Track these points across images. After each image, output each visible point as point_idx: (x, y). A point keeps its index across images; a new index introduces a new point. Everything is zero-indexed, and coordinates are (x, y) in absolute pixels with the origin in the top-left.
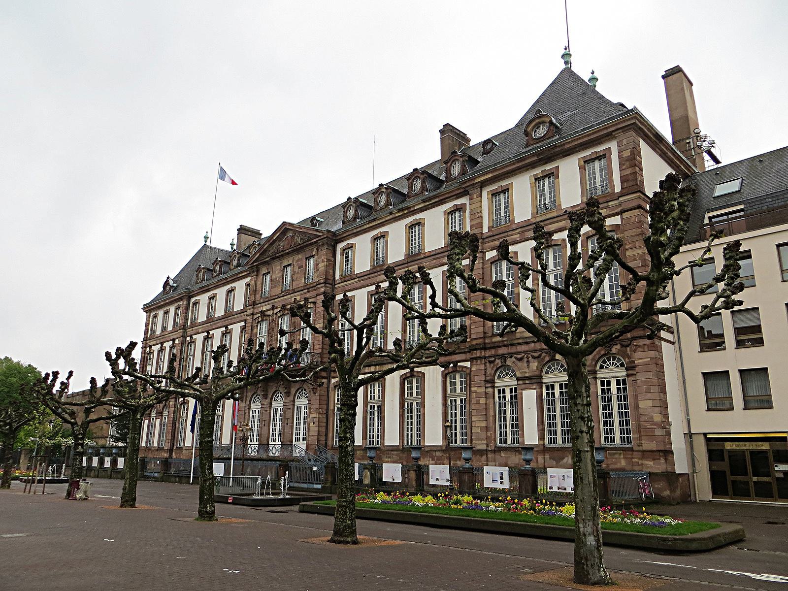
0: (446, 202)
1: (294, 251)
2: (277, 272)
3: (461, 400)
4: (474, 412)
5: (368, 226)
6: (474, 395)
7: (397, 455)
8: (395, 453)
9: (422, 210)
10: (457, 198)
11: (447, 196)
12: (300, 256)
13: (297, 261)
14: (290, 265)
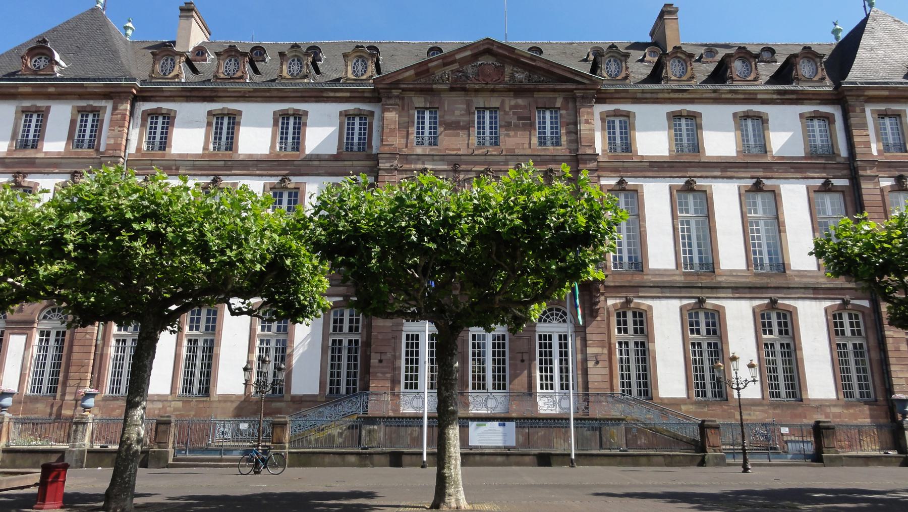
0: (802, 104)
1: (509, 90)
2: (457, 113)
3: (855, 345)
4: (892, 361)
5: (667, 96)
6: (889, 341)
7: (762, 411)
8: (761, 408)
9: (764, 102)
10: (820, 104)
11: (811, 96)
12: (520, 101)
13: (511, 108)
14: (491, 109)
